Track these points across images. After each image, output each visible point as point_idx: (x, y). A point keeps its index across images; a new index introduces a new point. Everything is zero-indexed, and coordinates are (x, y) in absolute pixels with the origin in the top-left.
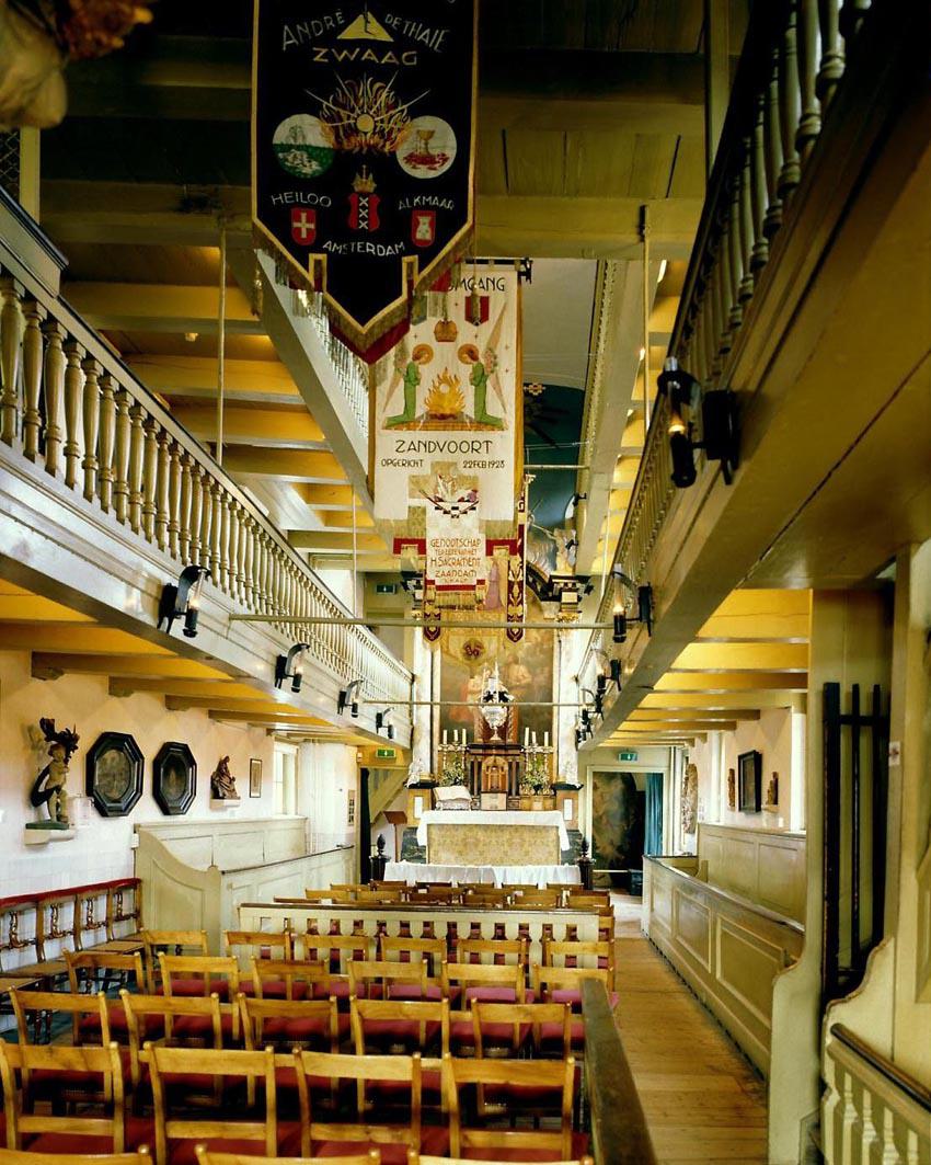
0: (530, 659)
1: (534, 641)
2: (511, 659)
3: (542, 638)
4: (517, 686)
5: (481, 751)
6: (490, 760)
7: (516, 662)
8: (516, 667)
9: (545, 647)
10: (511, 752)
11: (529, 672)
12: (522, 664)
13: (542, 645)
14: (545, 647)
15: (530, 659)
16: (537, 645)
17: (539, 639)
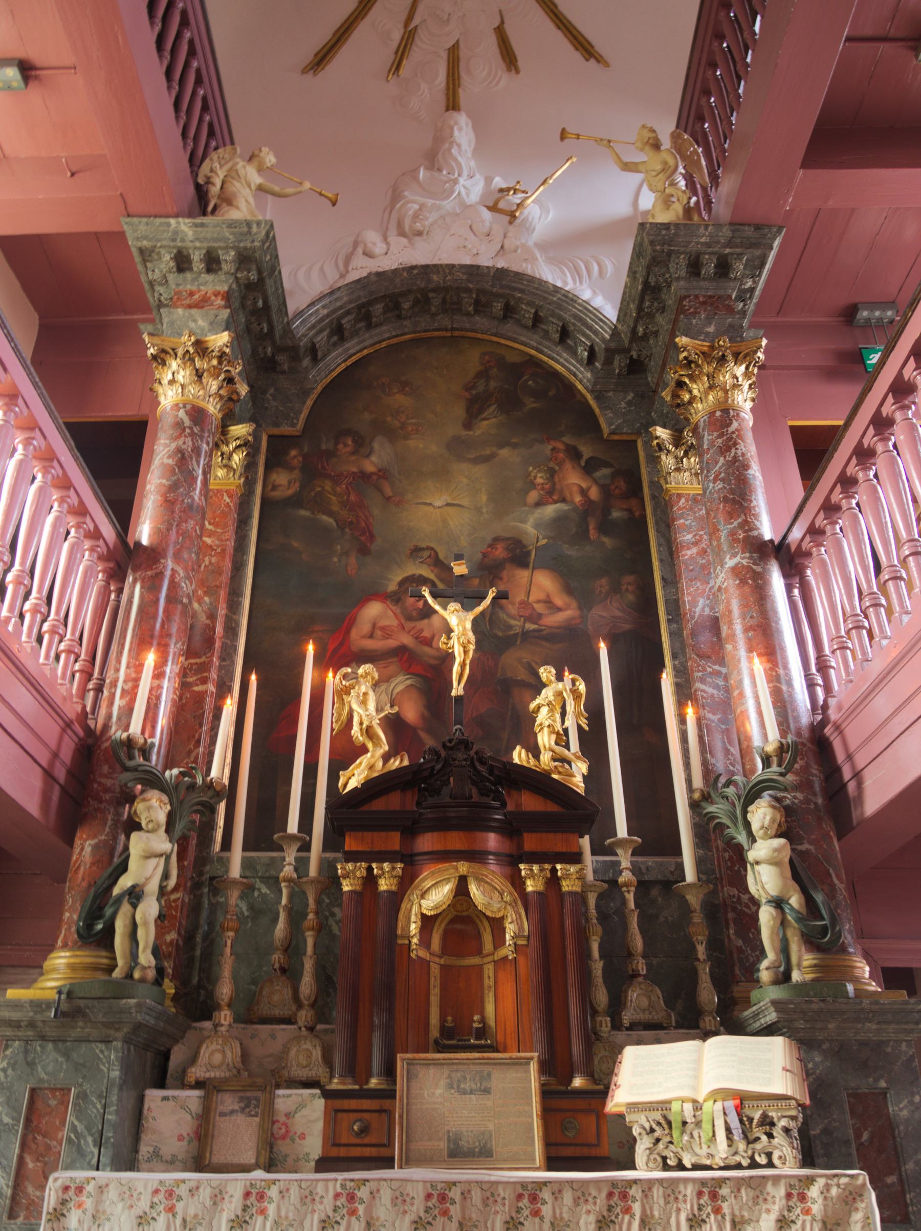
0: (572, 552)
1: (578, 499)
2: (500, 552)
3: (605, 490)
4: (526, 636)
5: (394, 841)
6: (435, 895)
7: (519, 555)
8: (523, 575)
9: (616, 514)
10: (531, 842)
11: (569, 590)
12: (541, 565)
13: (606, 511)
14: (616, 514)
15: (572, 552)
16: (589, 506)
17: (594, 493)
